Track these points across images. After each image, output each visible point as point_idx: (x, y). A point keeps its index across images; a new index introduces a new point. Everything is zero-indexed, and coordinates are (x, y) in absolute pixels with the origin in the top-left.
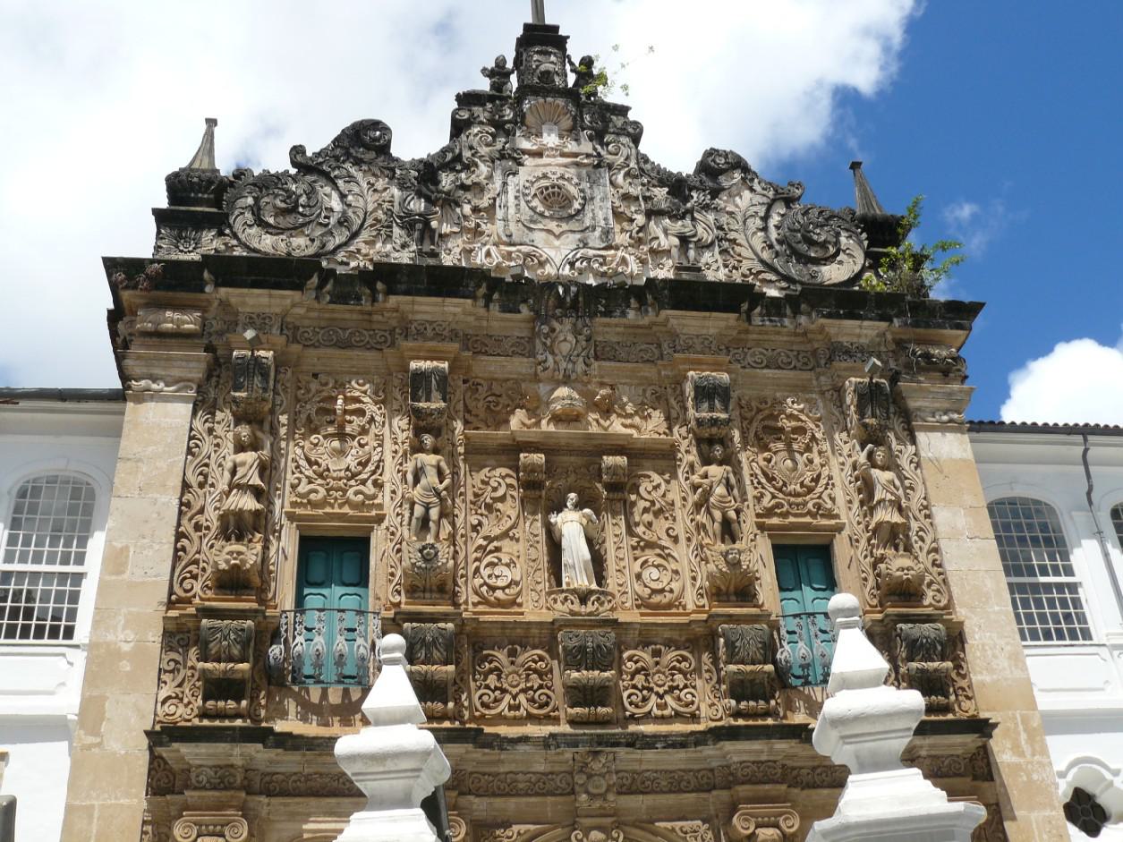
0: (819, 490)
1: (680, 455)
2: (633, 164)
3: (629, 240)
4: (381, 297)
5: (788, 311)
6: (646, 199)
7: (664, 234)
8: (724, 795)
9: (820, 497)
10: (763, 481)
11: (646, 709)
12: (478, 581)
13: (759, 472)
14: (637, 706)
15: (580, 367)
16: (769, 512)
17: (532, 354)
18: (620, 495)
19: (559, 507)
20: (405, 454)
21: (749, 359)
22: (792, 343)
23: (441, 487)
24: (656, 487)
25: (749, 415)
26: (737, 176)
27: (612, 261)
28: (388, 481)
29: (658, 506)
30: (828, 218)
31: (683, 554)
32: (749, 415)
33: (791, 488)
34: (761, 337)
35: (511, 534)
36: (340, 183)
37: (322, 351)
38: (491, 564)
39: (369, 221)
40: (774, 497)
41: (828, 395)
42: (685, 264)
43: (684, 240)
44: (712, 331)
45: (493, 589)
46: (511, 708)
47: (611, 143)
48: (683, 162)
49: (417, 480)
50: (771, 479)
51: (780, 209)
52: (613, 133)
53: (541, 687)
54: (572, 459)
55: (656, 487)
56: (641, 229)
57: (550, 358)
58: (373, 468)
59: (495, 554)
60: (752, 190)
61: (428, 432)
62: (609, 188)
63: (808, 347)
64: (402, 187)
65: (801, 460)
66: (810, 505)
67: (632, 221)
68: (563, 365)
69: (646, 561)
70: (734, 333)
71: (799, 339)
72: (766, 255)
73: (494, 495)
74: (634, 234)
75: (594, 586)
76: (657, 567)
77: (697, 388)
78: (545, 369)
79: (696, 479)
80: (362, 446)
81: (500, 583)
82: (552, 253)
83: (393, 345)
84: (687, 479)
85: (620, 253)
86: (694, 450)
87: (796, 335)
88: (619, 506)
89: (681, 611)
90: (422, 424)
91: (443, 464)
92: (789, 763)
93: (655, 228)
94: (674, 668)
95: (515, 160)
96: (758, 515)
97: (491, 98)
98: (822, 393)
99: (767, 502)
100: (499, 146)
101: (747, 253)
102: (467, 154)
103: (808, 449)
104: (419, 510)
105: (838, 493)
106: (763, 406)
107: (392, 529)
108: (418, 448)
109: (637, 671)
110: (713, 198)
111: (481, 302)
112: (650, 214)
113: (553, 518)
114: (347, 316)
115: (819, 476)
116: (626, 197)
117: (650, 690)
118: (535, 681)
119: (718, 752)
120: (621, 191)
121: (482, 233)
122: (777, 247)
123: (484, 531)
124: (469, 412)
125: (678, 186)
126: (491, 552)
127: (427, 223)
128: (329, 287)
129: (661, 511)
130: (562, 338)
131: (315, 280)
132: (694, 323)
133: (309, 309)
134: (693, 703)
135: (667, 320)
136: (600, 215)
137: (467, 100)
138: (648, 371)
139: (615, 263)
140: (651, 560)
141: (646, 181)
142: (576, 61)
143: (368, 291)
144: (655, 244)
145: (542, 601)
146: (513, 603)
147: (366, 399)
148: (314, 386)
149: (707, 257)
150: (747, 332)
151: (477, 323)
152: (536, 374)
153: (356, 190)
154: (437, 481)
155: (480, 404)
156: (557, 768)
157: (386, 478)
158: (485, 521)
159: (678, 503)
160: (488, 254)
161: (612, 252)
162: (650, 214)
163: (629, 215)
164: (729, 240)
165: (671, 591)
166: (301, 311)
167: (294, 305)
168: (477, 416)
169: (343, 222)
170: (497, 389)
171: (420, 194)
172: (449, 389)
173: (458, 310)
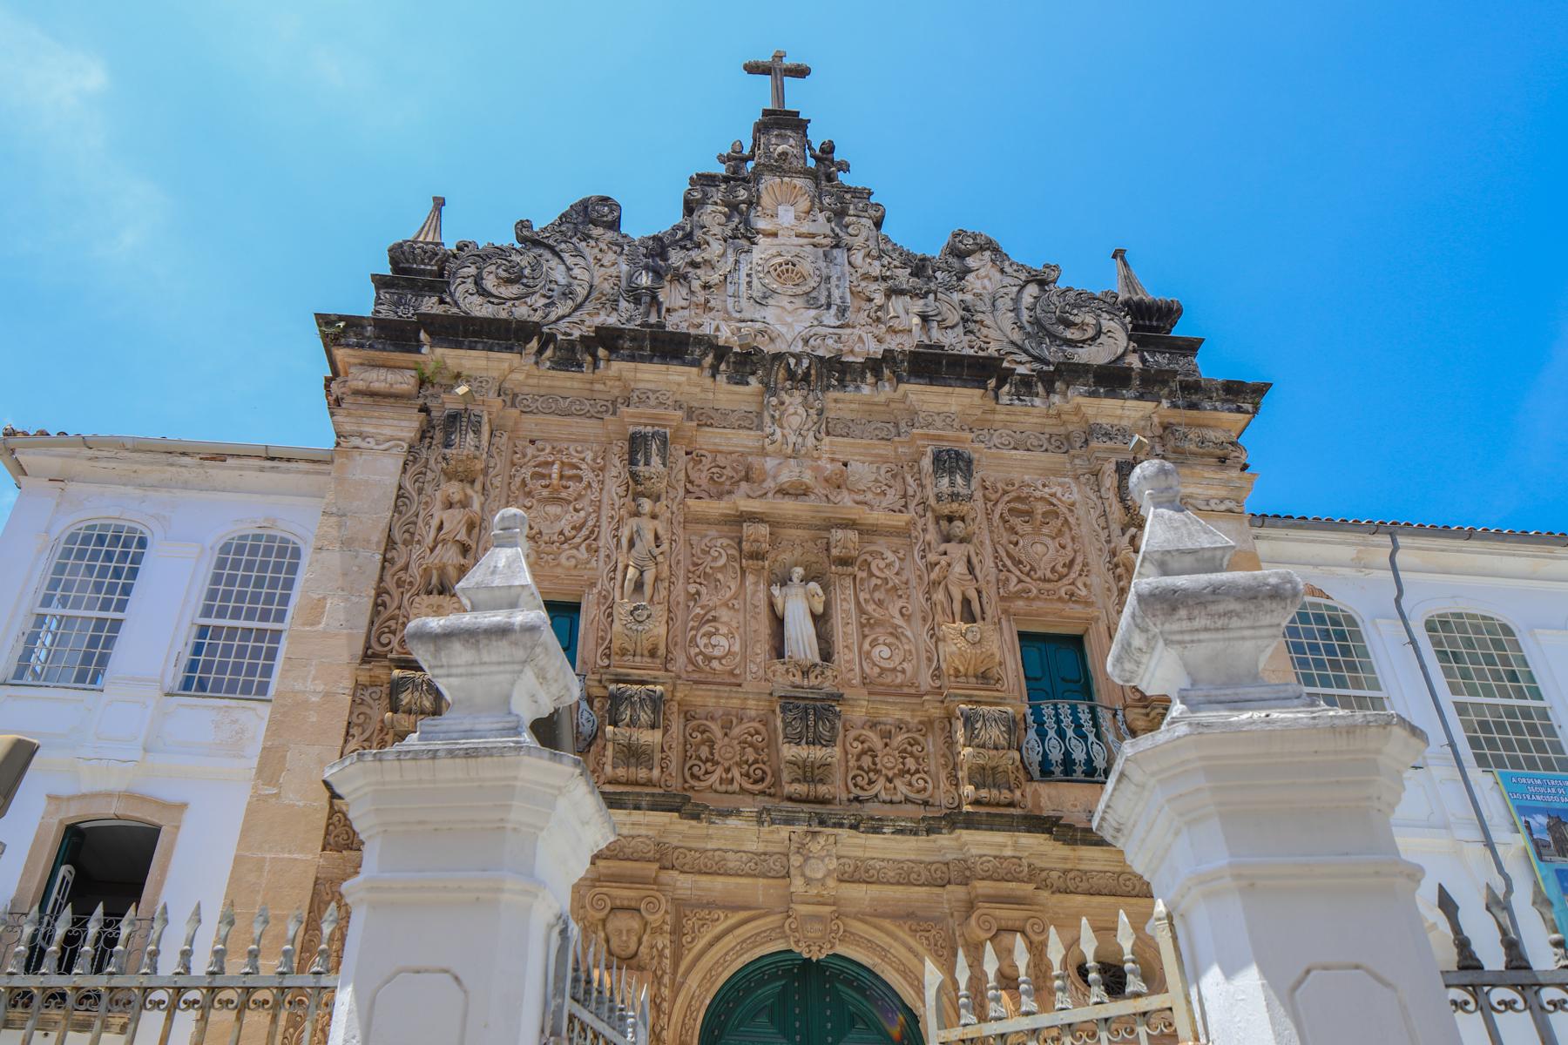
0: (1073, 575)
1: (914, 534)
2: (872, 244)
4: (602, 364)
5: (1040, 389)
6: (885, 279)
7: (905, 312)
8: (959, 892)
9: (1073, 583)
10: (1009, 563)
11: (873, 792)
13: (1004, 554)
14: (862, 788)
15: (810, 441)
16: (1018, 595)
17: (760, 427)
18: (850, 569)
19: (785, 581)
20: (621, 519)
21: (996, 441)
22: (1044, 425)
23: (656, 551)
24: (888, 566)
25: (994, 497)
29: (891, 584)
30: (1084, 300)
31: (916, 633)
32: (994, 497)
33: (1040, 574)
36: (566, 256)
37: (540, 417)
39: (595, 294)
40: (1020, 581)
41: (1083, 479)
43: (925, 318)
44: (953, 409)
45: (709, 659)
46: (721, 781)
48: (933, 248)
49: (632, 544)
50: (1018, 563)
51: (1032, 289)
53: (756, 761)
54: (799, 532)
55: (888, 566)
56: (880, 308)
57: (778, 431)
60: (1002, 271)
61: (644, 496)
62: (847, 268)
63: (1062, 430)
64: (632, 261)
65: (1053, 545)
66: (1063, 591)
67: (870, 300)
68: (792, 438)
69: (875, 639)
70: (979, 412)
71: (1054, 421)
72: (1017, 336)
75: (817, 660)
76: (889, 645)
77: (937, 459)
78: (773, 442)
79: (932, 557)
80: (576, 510)
81: (717, 653)
82: (784, 330)
83: (614, 413)
84: (923, 557)
85: (856, 331)
86: (931, 527)
87: (1048, 416)
88: (848, 582)
89: (913, 691)
90: (640, 488)
91: (661, 532)
92: (1039, 863)
94: (905, 751)
95: (749, 239)
96: (1002, 599)
97: (726, 180)
98: (1077, 478)
99: (1013, 586)
100: (732, 225)
101: (993, 334)
102: (698, 234)
103: (1060, 533)
105: (1094, 580)
106: (1010, 488)
108: (637, 514)
109: (863, 753)
110: (960, 279)
111: (707, 372)
112: (888, 295)
113: (776, 590)
114: (568, 384)
115: (1072, 562)
117: (877, 772)
118: (750, 755)
119: (954, 843)
121: (711, 309)
122: (1029, 329)
123: (704, 600)
124: (691, 482)
125: (920, 267)
126: (708, 621)
127: (654, 298)
128: (549, 353)
129: (895, 588)
130: (791, 410)
131: (534, 344)
132: (936, 399)
133: (528, 376)
134: (925, 789)
135: (905, 395)
136: (836, 293)
137: (705, 181)
138: (885, 449)
140: (881, 640)
142: (817, 147)
143: (589, 359)
145: (761, 673)
146: (731, 673)
147: (584, 466)
148: (531, 451)
150: (993, 411)
151: (702, 396)
152: (763, 448)
153: (582, 263)
155: (703, 475)
156: (770, 849)
158: (703, 590)
159: (914, 582)
160: (717, 329)
161: (849, 331)
162: (892, 292)
165: (903, 671)
166: (520, 377)
167: (512, 371)
169: (568, 293)
170: (721, 460)
171: (647, 268)
173: (683, 379)
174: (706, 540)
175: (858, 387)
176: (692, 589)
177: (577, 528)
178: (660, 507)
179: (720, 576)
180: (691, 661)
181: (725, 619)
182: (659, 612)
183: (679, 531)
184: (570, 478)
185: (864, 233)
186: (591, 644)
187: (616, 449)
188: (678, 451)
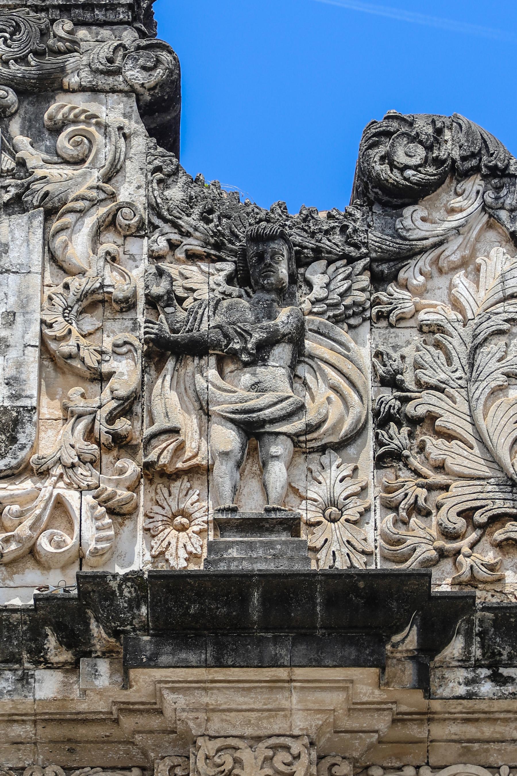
3: (82, 444)
6: (153, 302)
26: (466, 199)
27: (21, 515)
34: (471, 731)
42: (252, 506)
43: (253, 430)
44: (300, 723)
47: (65, 123)
52: (82, 89)
56: (127, 406)
67: (101, 378)
74: (102, 427)
85: (48, 488)
93: (167, 401)
101: (463, 459)
110: (379, 280)
116: (95, 301)
120: (77, 284)
139: (28, 522)
141: (162, 244)
144: (161, 453)
149: (331, 479)
150: (427, 717)
161: (27, 485)
162: (160, 352)
163: (92, 360)
164: (415, 422)
175: (24, 679)
185: (104, 151)
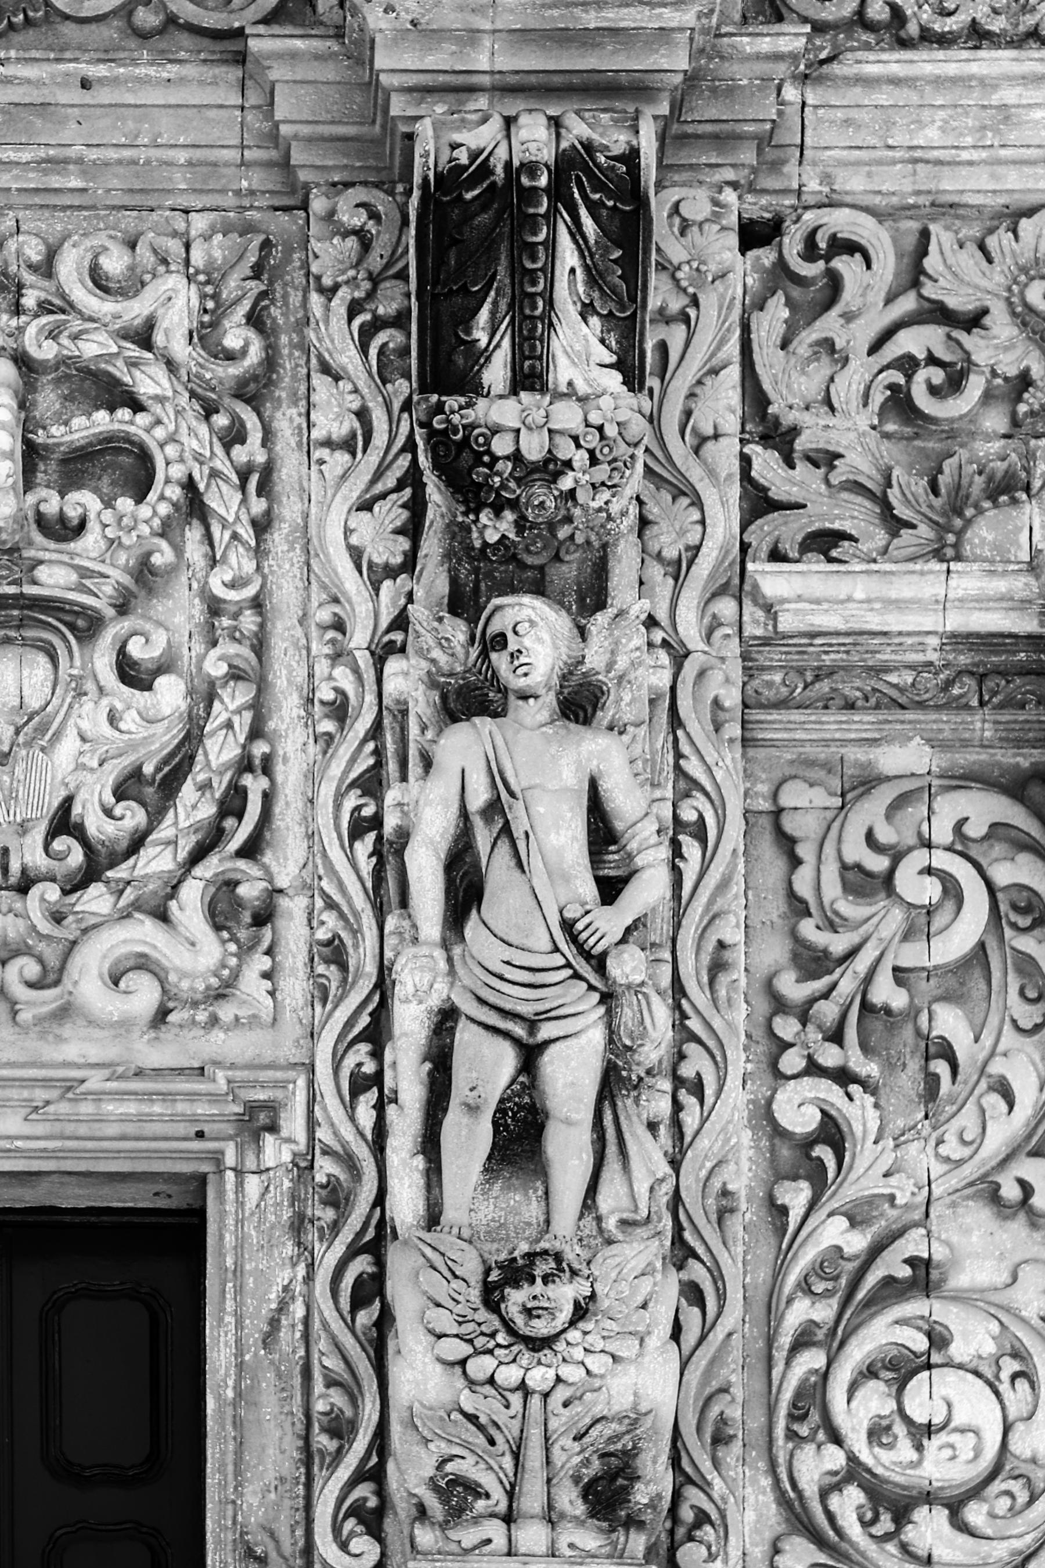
12: (815, 1465)
23: (607, 924)
28: (308, 888)
35: (1011, 1192)
38: (900, 1370)
58: (207, 810)
59: (915, 1307)
73: (912, 955)
91: (625, 801)
104: (486, 1067)
107: (325, 1168)
123: (865, 1174)
126: (892, 1290)
147: (150, 382)
154: (589, 890)
157: (286, 862)
168: (826, 460)
172: (659, 293)
174: (870, 813)
176: (798, 1109)
177: (153, 787)
178: (619, 649)
179: (950, 1023)
180: (799, 1518)
181: (975, 1273)
182: (634, 1273)
183: (720, 763)
184: (79, 465)
186: (274, 1452)
187: (330, 255)
188: (697, 232)
